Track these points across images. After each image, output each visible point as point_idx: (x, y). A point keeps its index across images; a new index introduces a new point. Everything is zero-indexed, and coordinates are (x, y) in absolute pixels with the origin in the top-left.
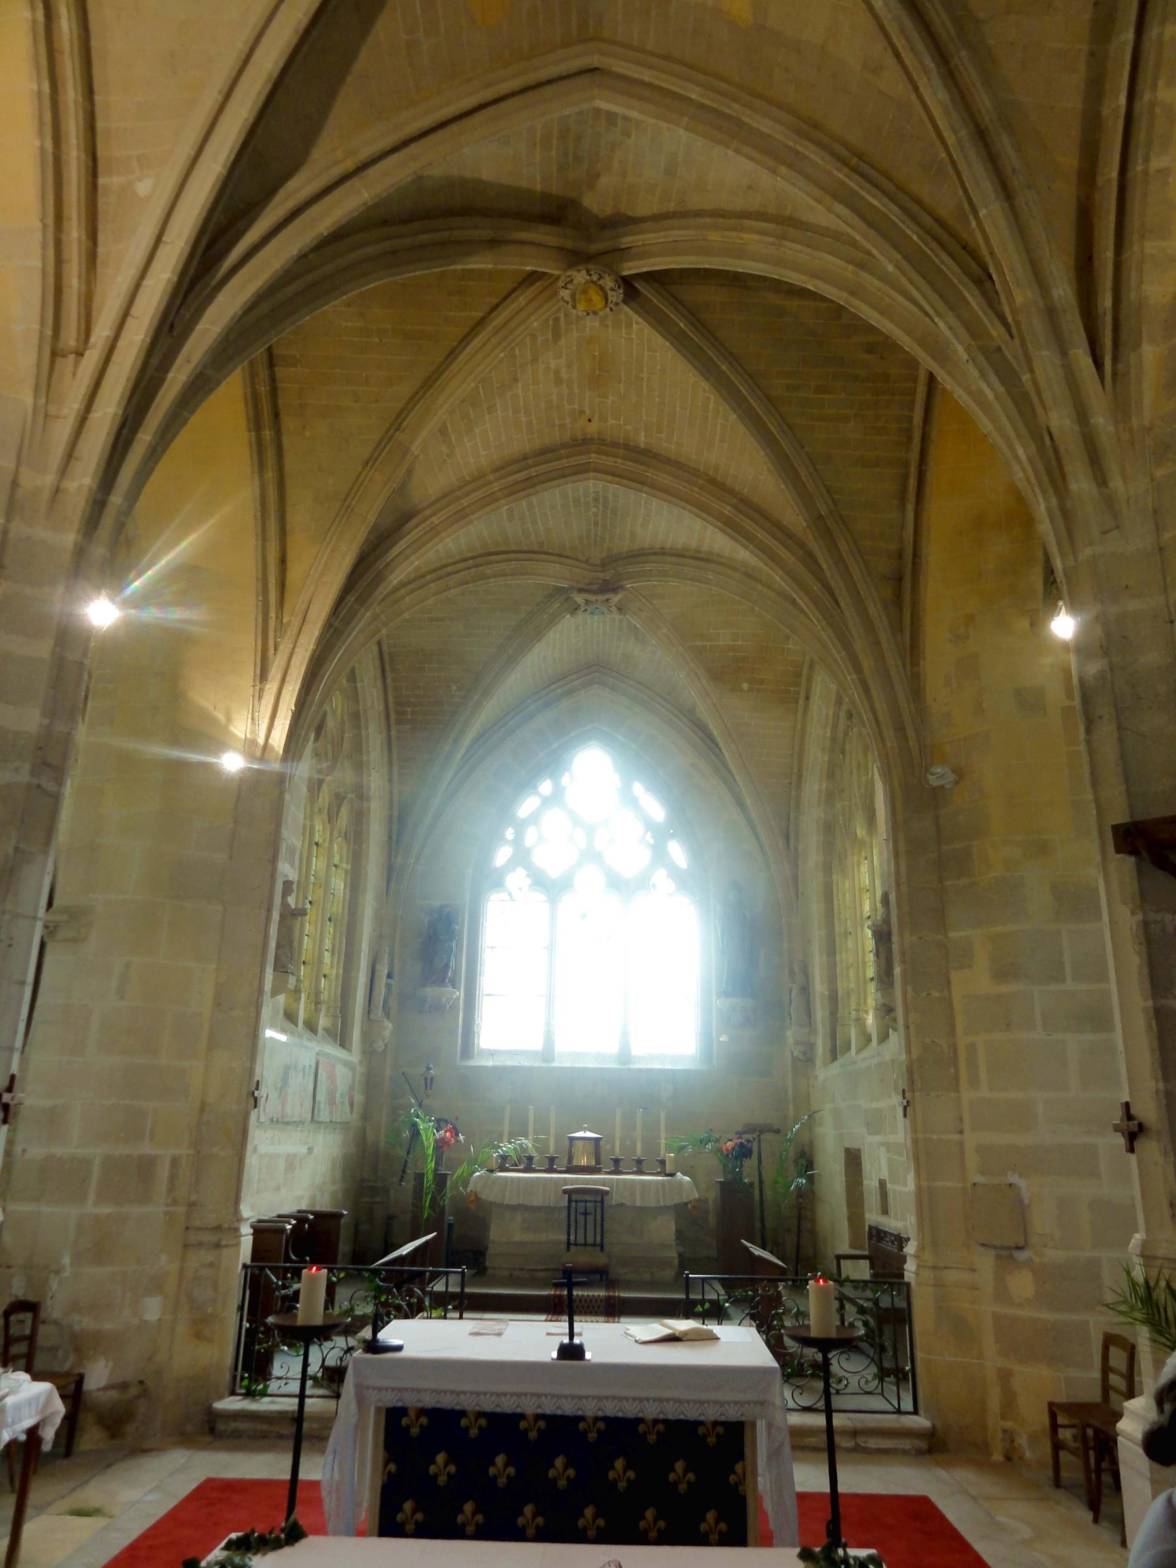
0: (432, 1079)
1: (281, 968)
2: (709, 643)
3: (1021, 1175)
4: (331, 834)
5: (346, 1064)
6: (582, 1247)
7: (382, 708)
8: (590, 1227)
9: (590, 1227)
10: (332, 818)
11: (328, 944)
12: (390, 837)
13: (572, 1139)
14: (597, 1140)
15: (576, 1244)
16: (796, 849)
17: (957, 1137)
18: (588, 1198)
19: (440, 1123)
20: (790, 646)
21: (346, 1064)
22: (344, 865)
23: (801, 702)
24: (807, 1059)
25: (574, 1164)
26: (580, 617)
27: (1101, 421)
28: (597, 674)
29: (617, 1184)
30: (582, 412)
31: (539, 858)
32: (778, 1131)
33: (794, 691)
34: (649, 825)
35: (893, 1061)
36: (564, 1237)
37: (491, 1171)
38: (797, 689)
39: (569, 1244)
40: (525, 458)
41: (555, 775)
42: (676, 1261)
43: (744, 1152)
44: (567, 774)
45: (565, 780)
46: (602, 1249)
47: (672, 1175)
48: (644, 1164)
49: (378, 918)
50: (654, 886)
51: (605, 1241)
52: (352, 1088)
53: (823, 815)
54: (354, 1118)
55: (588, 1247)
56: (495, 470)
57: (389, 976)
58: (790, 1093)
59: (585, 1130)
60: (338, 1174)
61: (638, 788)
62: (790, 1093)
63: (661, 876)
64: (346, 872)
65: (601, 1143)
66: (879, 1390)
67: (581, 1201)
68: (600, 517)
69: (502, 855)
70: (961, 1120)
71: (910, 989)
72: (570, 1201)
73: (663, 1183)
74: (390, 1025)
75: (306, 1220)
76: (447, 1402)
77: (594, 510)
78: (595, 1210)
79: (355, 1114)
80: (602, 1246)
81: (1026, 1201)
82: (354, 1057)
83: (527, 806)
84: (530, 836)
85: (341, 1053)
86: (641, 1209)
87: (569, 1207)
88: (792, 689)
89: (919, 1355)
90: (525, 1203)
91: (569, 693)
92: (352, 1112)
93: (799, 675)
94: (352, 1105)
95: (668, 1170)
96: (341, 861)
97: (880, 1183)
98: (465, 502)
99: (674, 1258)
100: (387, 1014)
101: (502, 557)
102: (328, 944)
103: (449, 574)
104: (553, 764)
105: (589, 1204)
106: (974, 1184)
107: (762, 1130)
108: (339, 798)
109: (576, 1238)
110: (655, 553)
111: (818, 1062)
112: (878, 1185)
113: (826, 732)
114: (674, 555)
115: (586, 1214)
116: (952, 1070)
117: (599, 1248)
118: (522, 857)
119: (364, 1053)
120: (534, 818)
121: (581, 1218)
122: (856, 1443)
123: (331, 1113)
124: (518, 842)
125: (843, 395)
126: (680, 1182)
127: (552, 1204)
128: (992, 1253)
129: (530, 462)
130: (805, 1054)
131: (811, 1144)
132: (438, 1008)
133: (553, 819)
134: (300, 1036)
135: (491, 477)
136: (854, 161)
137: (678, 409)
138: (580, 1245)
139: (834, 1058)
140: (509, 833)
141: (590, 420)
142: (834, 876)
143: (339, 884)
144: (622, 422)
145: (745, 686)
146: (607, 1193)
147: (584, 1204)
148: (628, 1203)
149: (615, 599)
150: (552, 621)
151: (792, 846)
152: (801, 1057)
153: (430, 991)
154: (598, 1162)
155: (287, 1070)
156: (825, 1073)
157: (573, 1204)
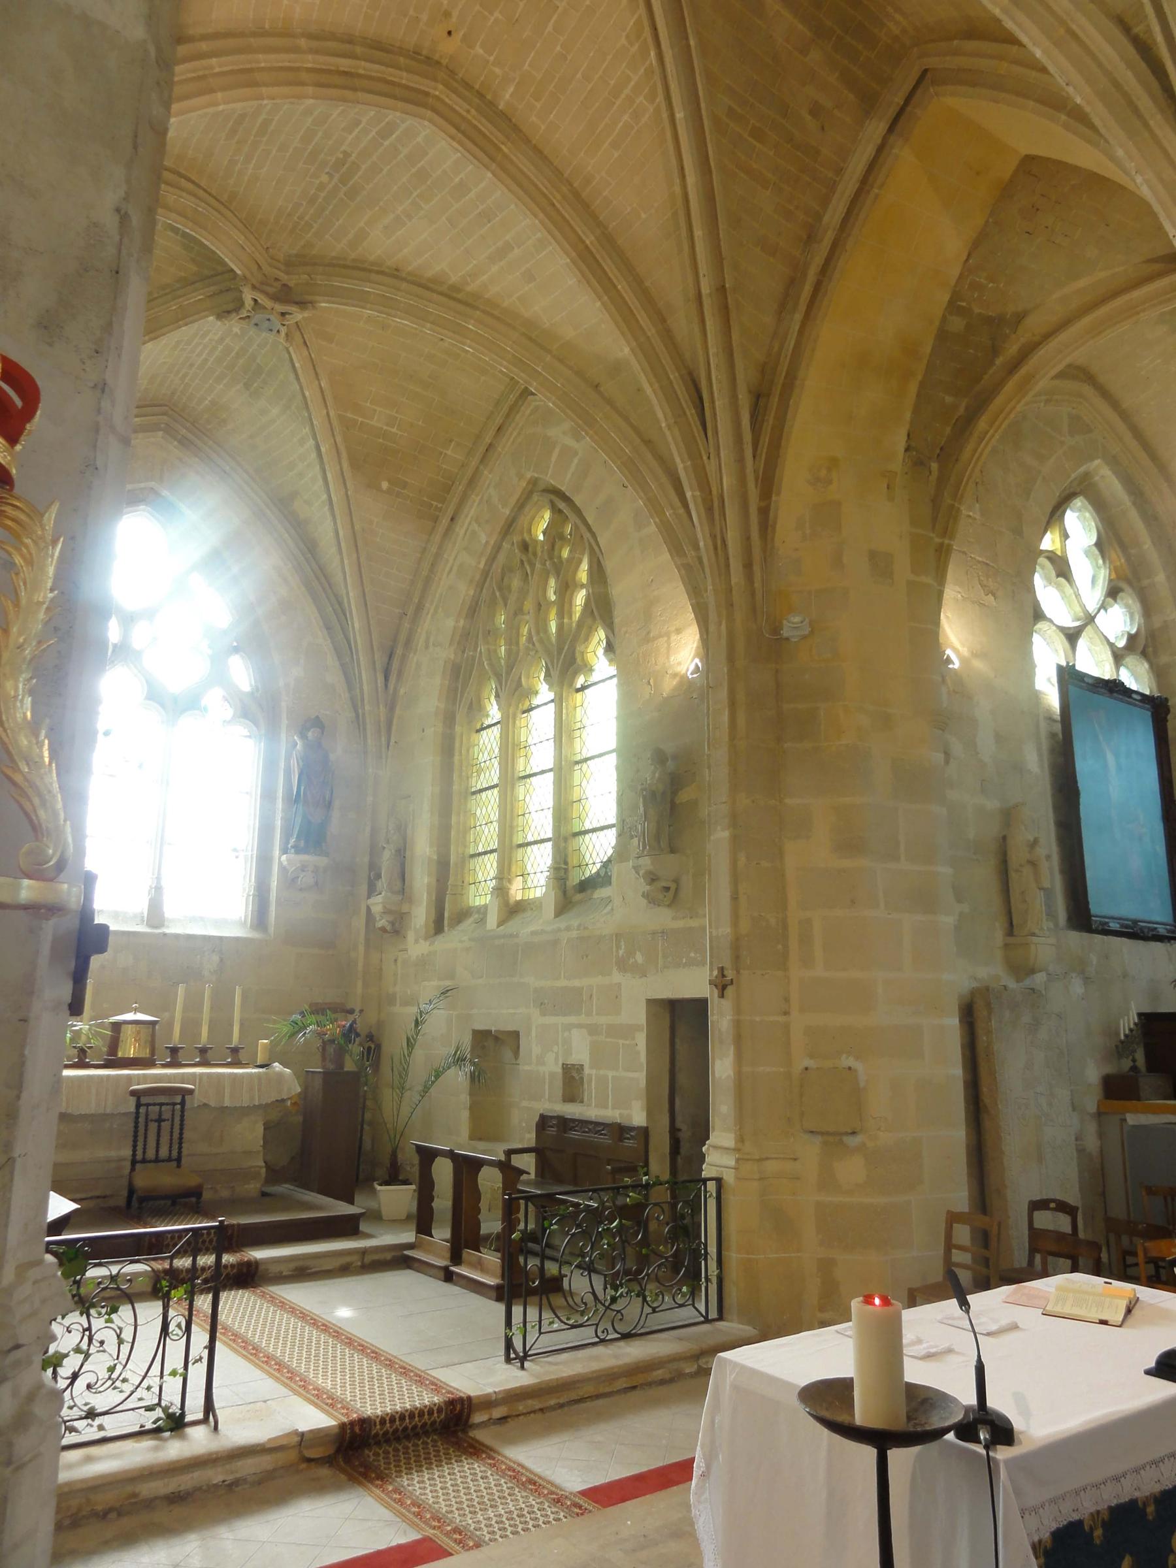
2: (360, 419)
3: (857, 1058)
6: (152, 1165)
8: (165, 1139)
9: (165, 1139)
15: (144, 1161)
16: (395, 689)
17: (781, 1019)
20: (449, 452)
23: (445, 521)
24: (397, 928)
25: (120, 1055)
26: (234, 325)
28: (165, 417)
29: (201, 1080)
30: (447, 14)
33: (436, 506)
35: (618, 936)
36: (127, 1152)
38: (440, 505)
39: (134, 1162)
40: (350, 40)
42: (264, 1170)
46: (179, 1166)
48: (181, 1053)
50: (205, 709)
51: (185, 1151)
53: (452, 657)
55: (160, 1164)
56: (310, 36)
59: (136, 1010)
63: (215, 699)
65: (157, 1027)
66: (690, 1302)
67: (154, 1104)
68: (323, 195)
70: (787, 1000)
71: (742, 859)
72: (138, 1105)
73: (259, 1075)
77: (324, 178)
78: (173, 1115)
80: (179, 1160)
81: (862, 1085)
86: (223, 1110)
87: (137, 1113)
88: (435, 503)
89: (733, 1256)
90: (69, 1111)
93: (448, 489)
97: (563, 1068)
98: (263, 60)
99: (261, 1167)
101: (191, 186)
105: (164, 1108)
106: (806, 1069)
109: (144, 1152)
110: (382, 273)
111: (411, 936)
112: (559, 1070)
113: (479, 563)
114: (413, 283)
115: (160, 1120)
116: (780, 947)
117: (174, 1164)
121: (153, 1127)
122: (699, 1367)
125: (771, 153)
126: (280, 1075)
127: (108, 1111)
128: (818, 1140)
130: (393, 924)
137: (579, 76)
138: (150, 1162)
141: (449, 33)
142: (458, 729)
144: (492, 58)
145: (385, 485)
146: (191, 1092)
147: (158, 1107)
148: (212, 1104)
149: (298, 315)
150: (183, 317)
151: (391, 686)
152: (388, 928)
154: (153, 1053)
156: (416, 946)
157: (142, 1110)
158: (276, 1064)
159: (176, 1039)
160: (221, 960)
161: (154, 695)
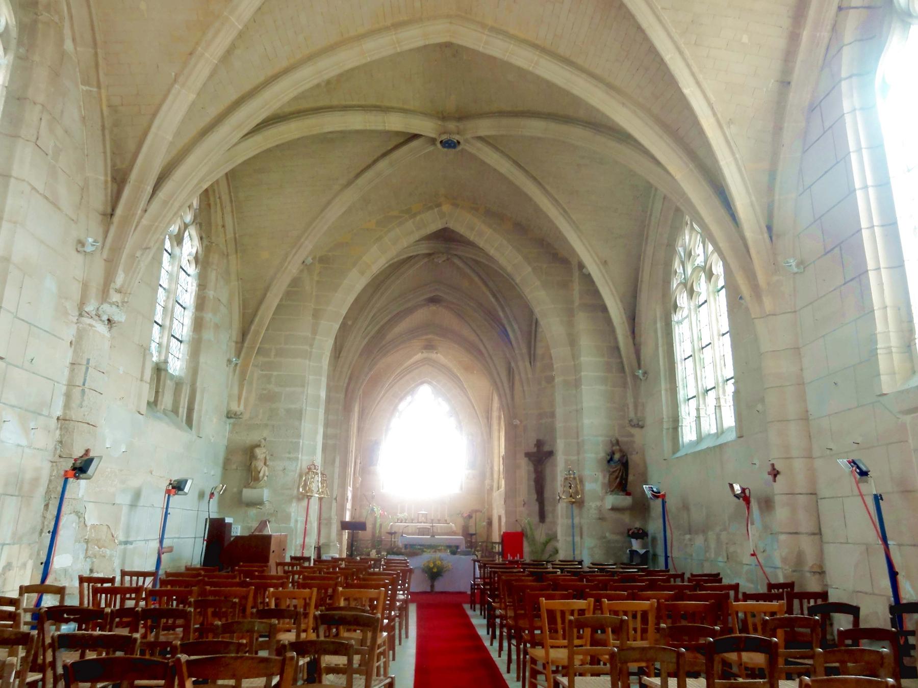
24: (491, 489)
27: (530, 376)
32: (481, 512)
43: (470, 517)
58: (486, 499)
62: (486, 499)
95: (448, 522)
104: (412, 391)
107: (476, 511)
119: (353, 488)
131: (492, 515)
139: (498, 489)
154: (427, 520)
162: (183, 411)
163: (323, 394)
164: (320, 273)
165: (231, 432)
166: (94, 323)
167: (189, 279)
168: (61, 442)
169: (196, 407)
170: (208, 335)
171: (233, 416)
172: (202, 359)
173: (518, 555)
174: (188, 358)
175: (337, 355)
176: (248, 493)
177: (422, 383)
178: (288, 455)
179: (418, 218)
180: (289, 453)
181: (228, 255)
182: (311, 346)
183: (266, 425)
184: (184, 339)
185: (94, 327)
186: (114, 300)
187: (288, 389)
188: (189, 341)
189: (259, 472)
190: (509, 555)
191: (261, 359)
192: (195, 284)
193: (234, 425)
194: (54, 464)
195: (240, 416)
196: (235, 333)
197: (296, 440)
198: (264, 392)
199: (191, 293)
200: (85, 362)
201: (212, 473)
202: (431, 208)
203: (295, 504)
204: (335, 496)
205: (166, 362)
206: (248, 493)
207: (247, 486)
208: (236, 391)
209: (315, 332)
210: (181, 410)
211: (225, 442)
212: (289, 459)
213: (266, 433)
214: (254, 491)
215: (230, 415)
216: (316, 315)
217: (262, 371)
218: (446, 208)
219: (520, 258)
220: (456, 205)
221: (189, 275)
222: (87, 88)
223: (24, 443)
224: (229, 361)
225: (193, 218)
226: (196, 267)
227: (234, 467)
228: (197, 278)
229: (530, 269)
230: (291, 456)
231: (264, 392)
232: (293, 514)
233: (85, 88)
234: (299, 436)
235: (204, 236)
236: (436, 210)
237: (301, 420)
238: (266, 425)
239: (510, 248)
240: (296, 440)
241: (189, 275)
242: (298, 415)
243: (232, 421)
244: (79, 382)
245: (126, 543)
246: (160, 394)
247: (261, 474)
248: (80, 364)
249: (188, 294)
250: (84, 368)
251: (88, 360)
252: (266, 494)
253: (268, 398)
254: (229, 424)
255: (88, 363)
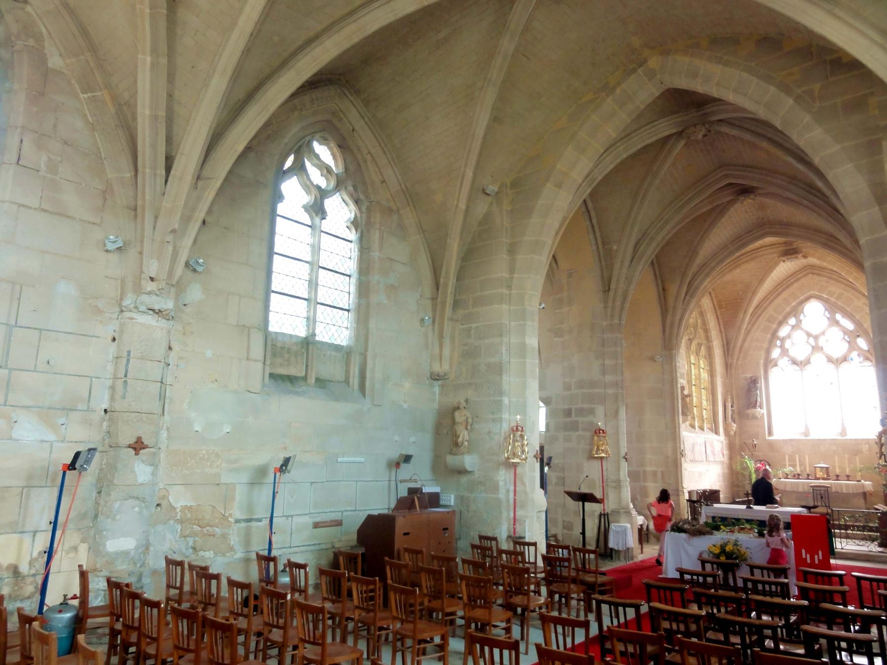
0: (755, 445)
1: (684, 414)
4: (699, 360)
5: (718, 441)
7: (712, 306)
10: (697, 354)
11: (704, 397)
12: (724, 352)
13: (815, 467)
14: (827, 468)
18: (822, 489)
19: (756, 462)
21: (718, 441)
22: (706, 368)
31: (792, 353)
34: (845, 332)
37: (780, 479)
41: (796, 316)
44: (802, 314)
45: (802, 317)
47: (859, 481)
49: (725, 385)
50: (852, 359)
52: (722, 449)
54: (726, 459)
57: (732, 407)
60: (721, 478)
61: (838, 317)
63: (854, 355)
64: (708, 370)
69: (776, 353)
72: (813, 490)
73: (855, 485)
74: (735, 425)
75: (707, 491)
76: (724, 516)
79: (725, 457)
82: (722, 437)
83: (783, 332)
84: (788, 344)
85: (713, 436)
87: (813, 492)
91: (796, 281)
92: (724, 457)
94: (723, 455)
96: (705, 366)
100: (734, 421)
102: (704, 397)
103: (724, 270)
104: (796, 311)
108: (699, 345)
118: (785, 352)
120: (789, 336)
123: (714, 458)
124: (782, 347)
127: (807, 491)
129: (744, 237)
132: (754, 417)
133: (799, 335)
134: (697, 433)
135: (730, 246)
136: (808, 189)
140: (778, 343)
143: (705, 375)
148: (839, 491)
153: (751, 411)
155: (693, 445)
158: (862, 481)
159: (838, 471)
160: (870, 447)
161: (830, 360)
162: (355, 382)
163: (532, 341)
164: (513, 200)
165: (441, 394)
166: (134, 315)
167: (352, 245)
168: (109, 432)
169: (368, 375)
170: (379, 297)
171: (437, 378)
172: (372, 325)
173: (820, 553)
174: (355, 326)
175: (607, 289)
176: (450, 460)
177: (807, 299)
178: (491, 416)
179: (618, 91)
180: (493, 413)
181: (398, 210)
182: (509, 287)
183: (470, 384)
184: (351, 307)
185: (134, 319)
186: (149, 289)
187: (486, 341)
188: (355, 309)
189: (459, 437)
190: (803, 551)
191: (461, 312)
192: (356, 250)
193: (442, 386)
194: (105, 453)
195: (445, 377)
196: (428, 291)
197: (499, 398)
198: (466, 348)
199: (354, 259)
200: (125, 354)
201: (413, 439)
202: (634, 70)
203: (504, 472)
204: (623, 454)
205: (314, 335)
206: (450, 460)
207: (451, 453)
208: (437, 350)
209: (512, 271)
210: (351, 380)
211: (436, 406)
212: (494, 420)
213: (470, 393)
214: (456, 457)
215: (435, 377)
216: (512, 250)
217: (463, 325)
218: (654, 62)
219: (772, 89)
220: (666, 53)
221: (351, 242)
222: (89, 94)
223: (52, 437)
224: (422, 320)
225: (336, 183)
226: (356, 232)
227: (445, 431)
228: (358, 243)
229: (791, 102)
230: (495, 416)
231: (466, 348)
232: (501, 483)
233: (86, 96)
234: (501, 393)
235: (362, 197)
236: (640, 71)
237: (501, 375)
238: (470, 384)
239: (755, 80)
240: (499, 398)
241: (351, 242)
242: (498, 369)
243: (440, 382)
244: (121, 374)
245: (249, 520)
246: (309, 368)
247: (460, 440)
248: (121, 357)
249: (352, 261)
250: (124, 361)
251: (129, 353)
252: (469, 461)
253: (469, 354)
254: (439, 386)
255: (129, 355)
